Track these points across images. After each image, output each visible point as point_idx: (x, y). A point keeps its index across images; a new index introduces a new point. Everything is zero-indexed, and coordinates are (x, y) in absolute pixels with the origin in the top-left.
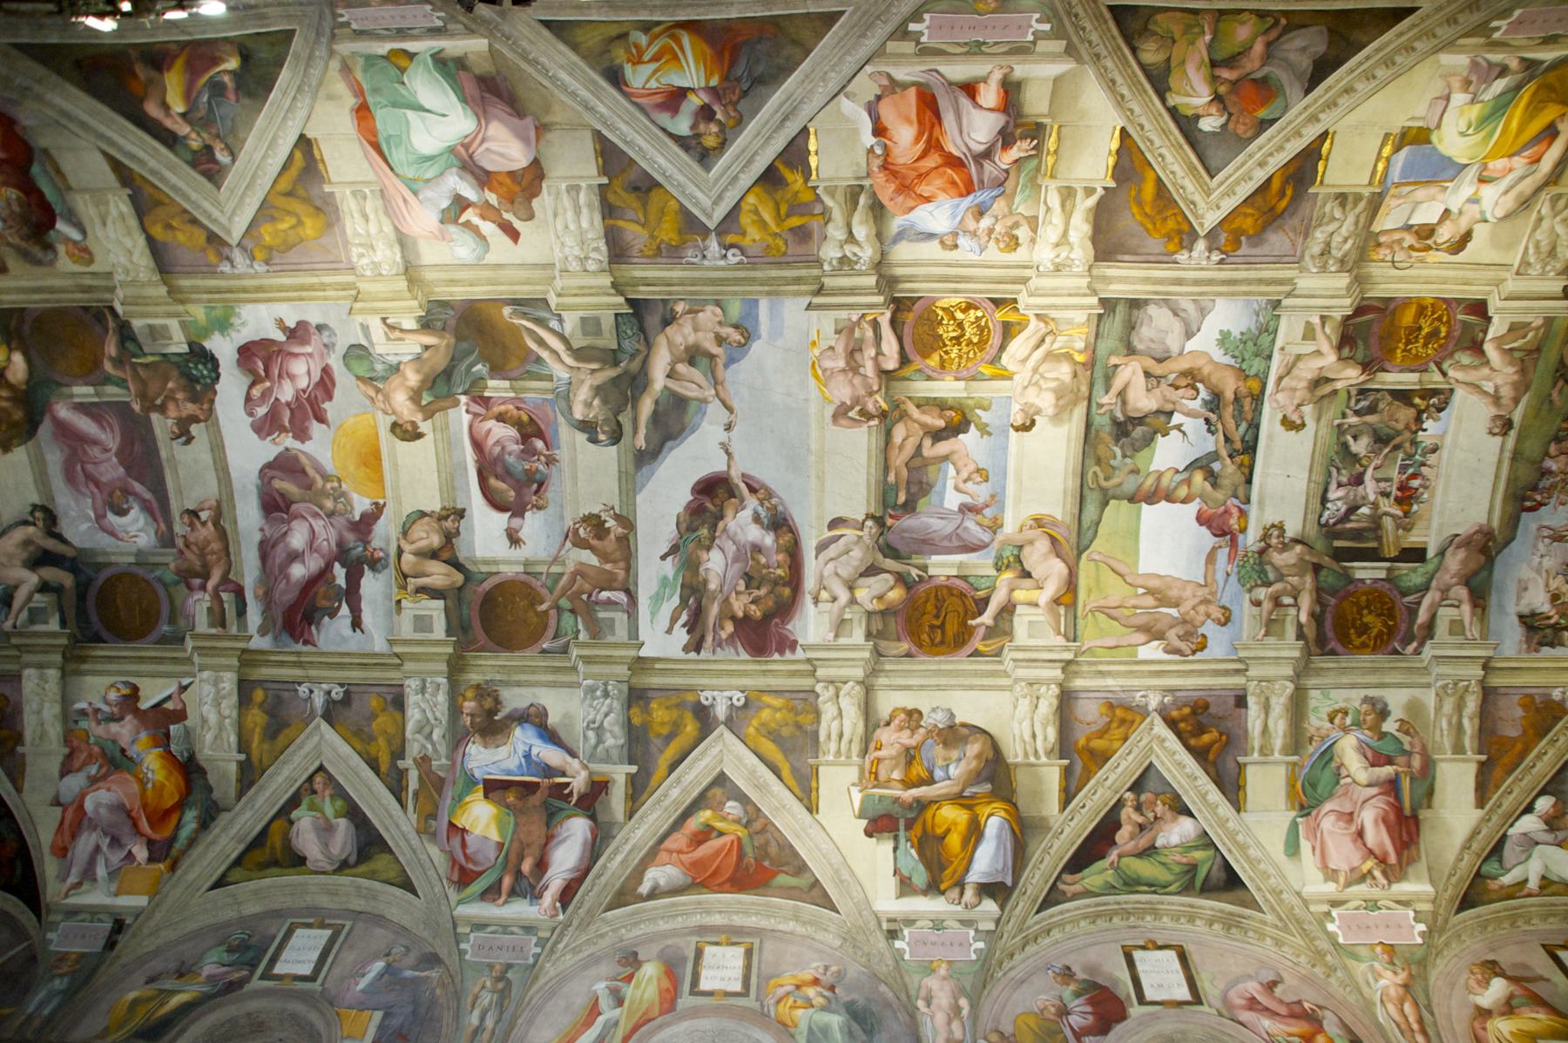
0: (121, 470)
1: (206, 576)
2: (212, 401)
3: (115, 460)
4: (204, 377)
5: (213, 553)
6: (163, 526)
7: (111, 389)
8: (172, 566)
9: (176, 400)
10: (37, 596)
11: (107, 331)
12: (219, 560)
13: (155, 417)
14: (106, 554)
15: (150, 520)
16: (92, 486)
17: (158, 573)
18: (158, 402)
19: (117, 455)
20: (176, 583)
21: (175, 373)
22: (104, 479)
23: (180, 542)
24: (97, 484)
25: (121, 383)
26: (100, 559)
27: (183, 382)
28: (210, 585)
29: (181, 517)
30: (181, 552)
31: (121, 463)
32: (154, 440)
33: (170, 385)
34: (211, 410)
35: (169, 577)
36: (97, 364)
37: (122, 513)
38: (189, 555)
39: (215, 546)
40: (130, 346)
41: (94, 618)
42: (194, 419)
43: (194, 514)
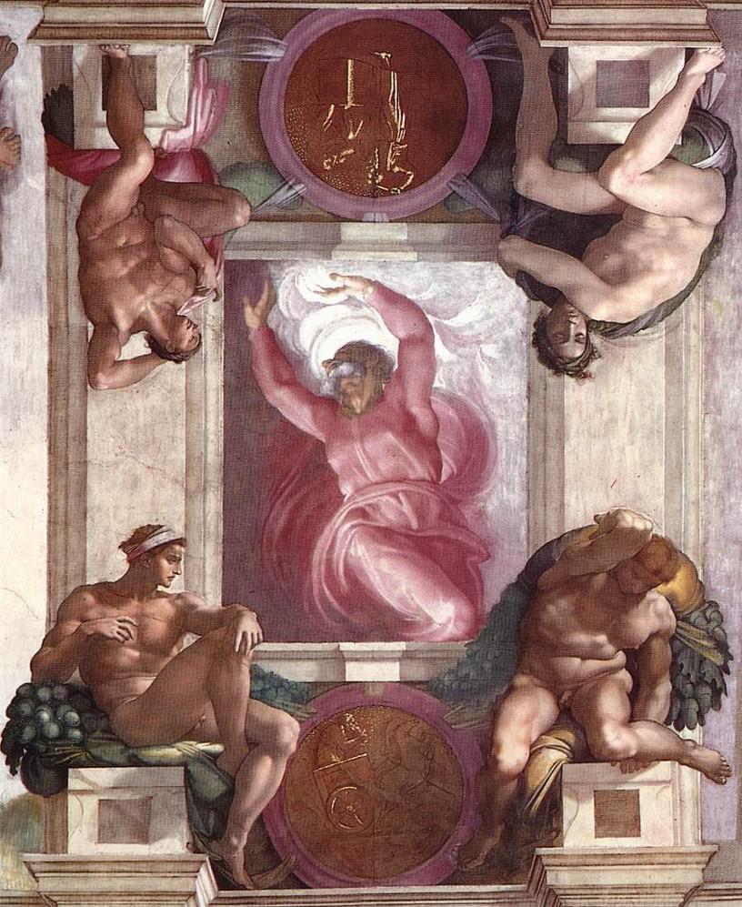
0: (335, 463)
1: (151, 189)
2: (51, 639)
3: (347, 490)
4: (54, 704)
5: (125, 251)
6: (251, 318)
7: (301, 672)
8: (241, 215)
9: (143, 645)
10: (620, 134)
11: (260, 821)
12: (109, 235)
13: (211, 600)
14: (414, 245)
15: (284, 333)
16: (423, 419)
17: (283, 195)
18: (189, 640)
19: (339, 499)
20: (235, 169)
21: (123, 713)
22: (390, 437)
23: (213, 276)
24: (408, 427)
25: (268, 687)
26: (437, 232)
27: (111, 691)
28: (143, 166)
29: (198, 339)
30: (212, 250)
31: (331, 479)
32: (229, 542)
33: (144, 683)
34: (59, 616)
35: (255, 186)
36: (315, 739)
37: (360, 354)
38: (192, 245)
39: (118, 268)
40: (213, 786)
41: (477, 83)
42: (109, 593)
43: (162, 350)
